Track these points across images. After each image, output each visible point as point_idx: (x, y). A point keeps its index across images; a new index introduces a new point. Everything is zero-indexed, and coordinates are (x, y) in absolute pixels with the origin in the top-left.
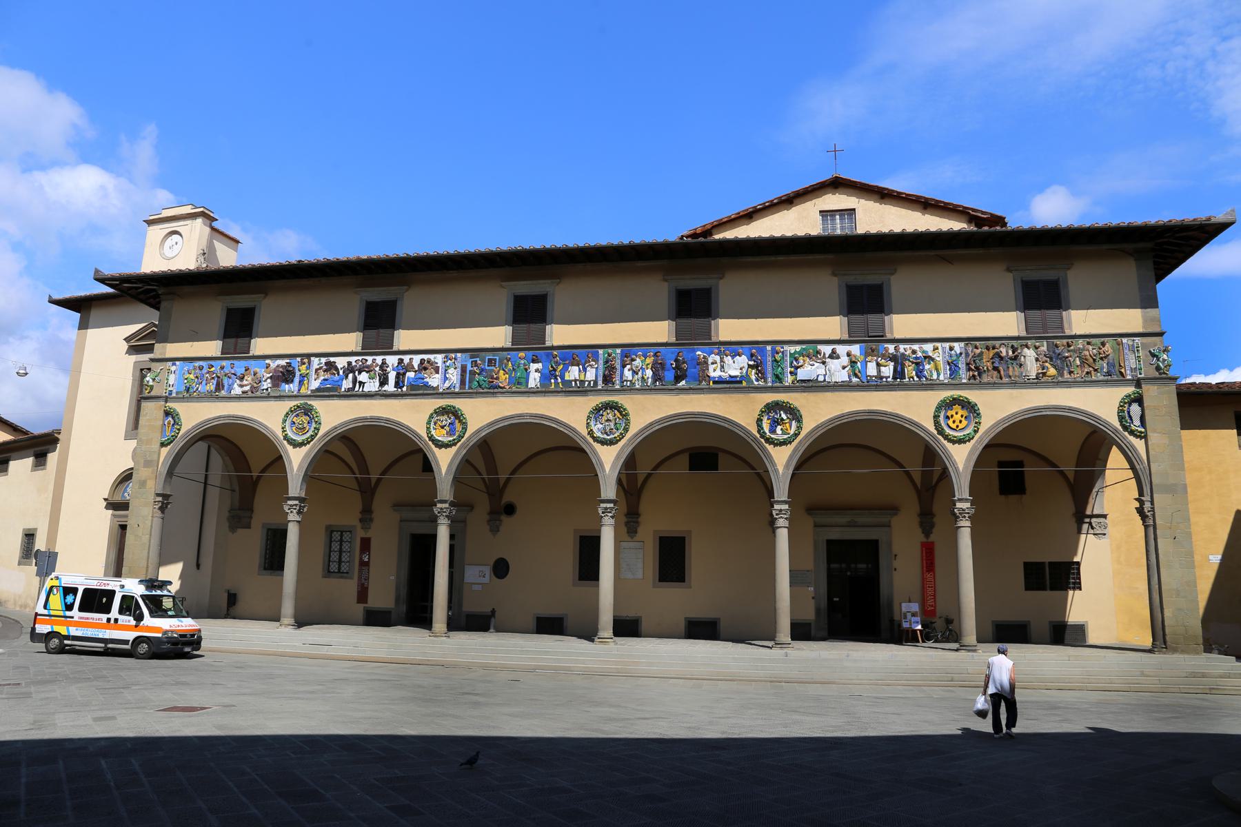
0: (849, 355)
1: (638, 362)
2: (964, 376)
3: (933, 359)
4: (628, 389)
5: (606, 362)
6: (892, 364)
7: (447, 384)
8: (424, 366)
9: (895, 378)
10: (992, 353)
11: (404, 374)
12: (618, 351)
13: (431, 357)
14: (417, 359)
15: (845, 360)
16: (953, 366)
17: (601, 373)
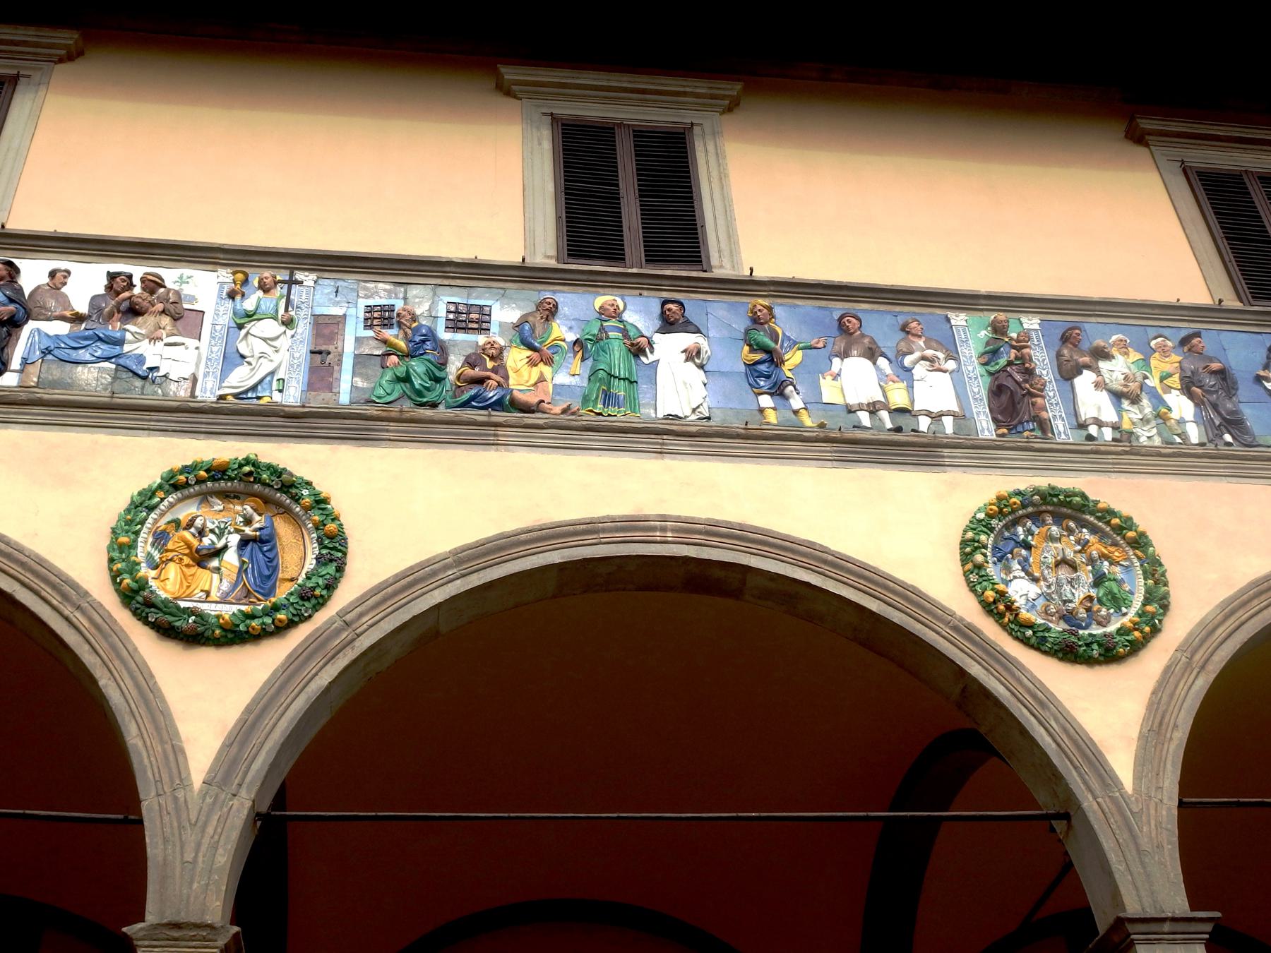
1: (1117, 368)
4: (1124, 452)
5: (990, 354)
7: (240, 378)
8: (124, 304)
11: (14, 324)
12: (1031, 323)
13: (171, 275)
14: (86, 282)
17: (979, 387)
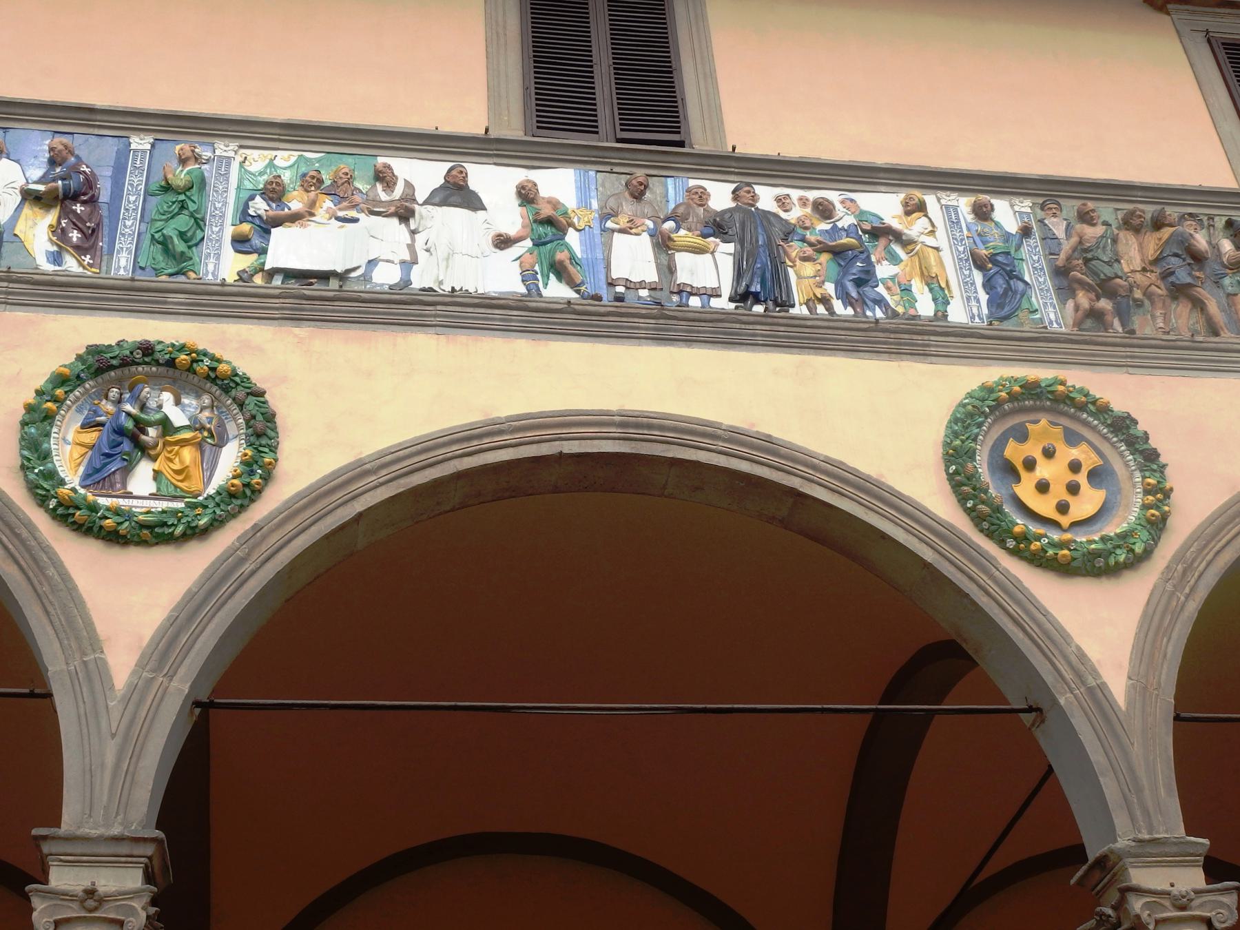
0: (526, 195)
2: (1048, 309)
3: (906, 243)
6: (725, 251)
9: (742, 297)
10: (1152, 243)
15: (512, 219)
16: (998, 270)
